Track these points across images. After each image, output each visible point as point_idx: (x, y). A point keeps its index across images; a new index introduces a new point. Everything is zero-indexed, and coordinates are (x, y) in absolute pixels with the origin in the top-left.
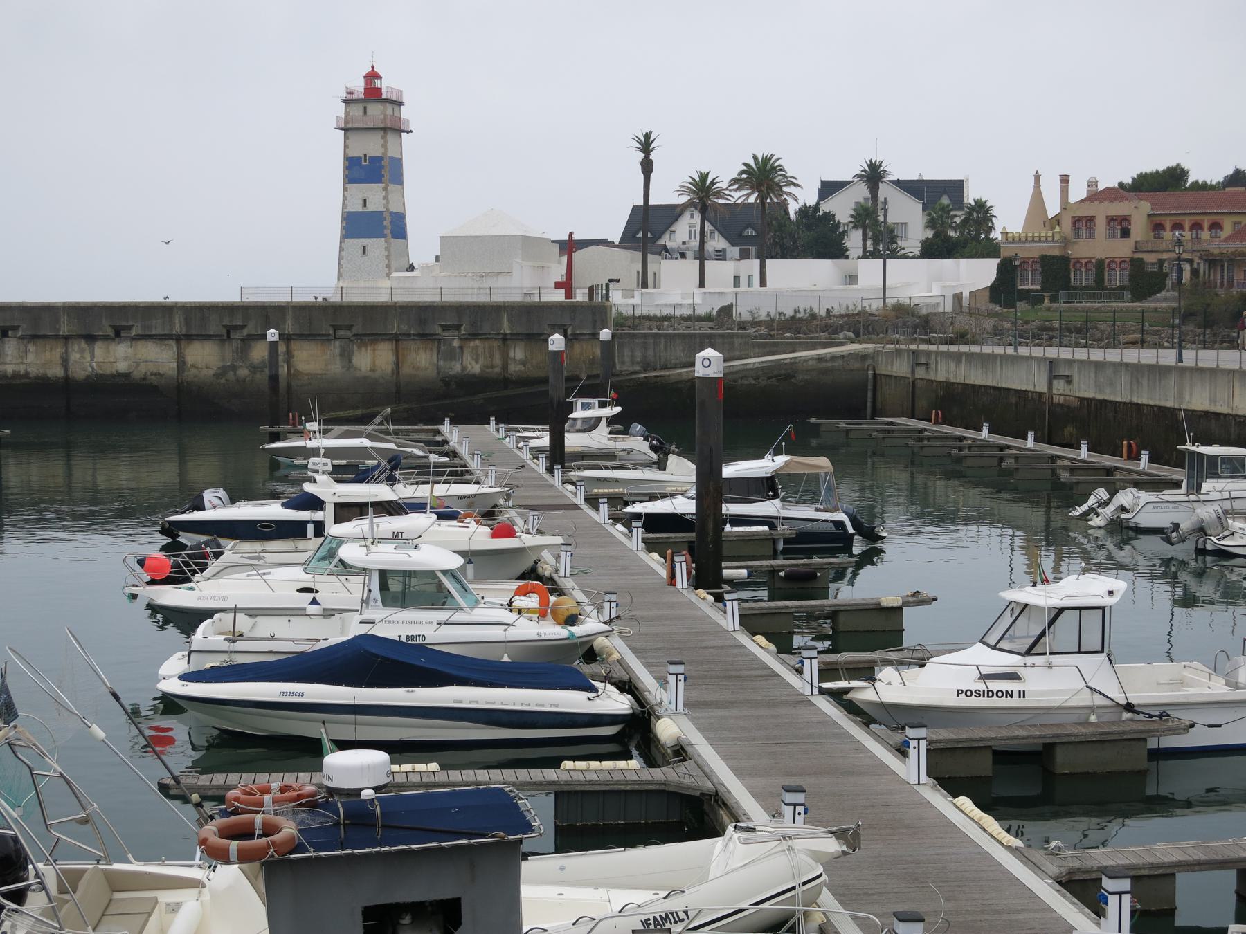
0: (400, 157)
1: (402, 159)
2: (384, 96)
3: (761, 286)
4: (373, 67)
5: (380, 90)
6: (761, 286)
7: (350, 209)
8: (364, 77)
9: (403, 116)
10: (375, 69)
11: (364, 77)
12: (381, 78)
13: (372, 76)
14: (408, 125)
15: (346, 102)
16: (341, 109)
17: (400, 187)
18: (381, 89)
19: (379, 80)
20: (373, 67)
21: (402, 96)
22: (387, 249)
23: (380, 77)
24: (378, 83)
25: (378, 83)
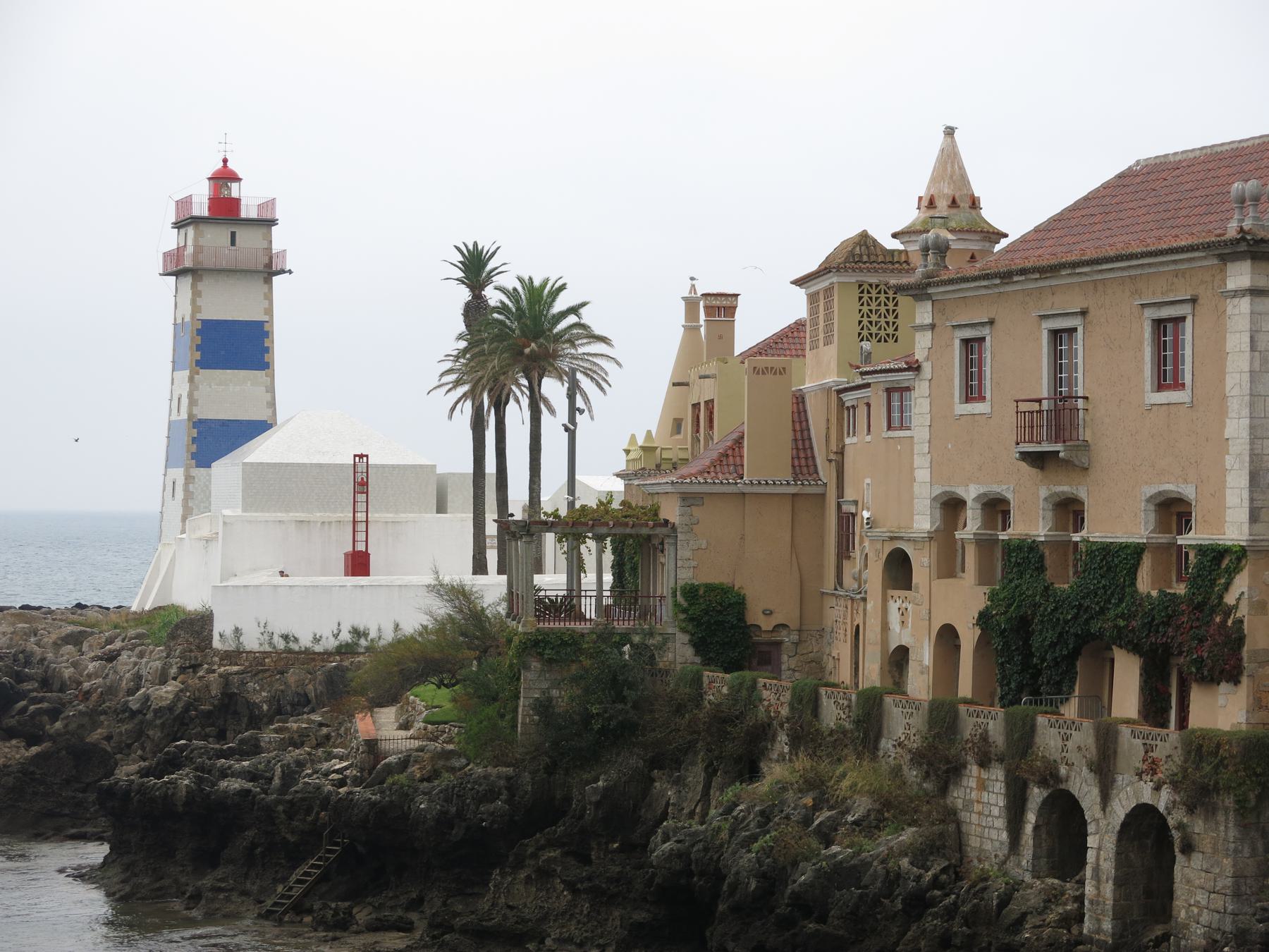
0: (266, 318)
1: (271, 322)
2: (243, 215)
3: (475, 573)
4: (225, 161)
5: (236, 203)
6: (475, 573)
7: (174, 417)
9: (276, 247)
10: (229, 164)
11: (210, 179)
13: (224, 177)
15: (179, 225)
16: (171, 240)
17: (259, 374)
20: (225, 161)
21: (273, 209)
22: (186, 490)
23: (236, 178)
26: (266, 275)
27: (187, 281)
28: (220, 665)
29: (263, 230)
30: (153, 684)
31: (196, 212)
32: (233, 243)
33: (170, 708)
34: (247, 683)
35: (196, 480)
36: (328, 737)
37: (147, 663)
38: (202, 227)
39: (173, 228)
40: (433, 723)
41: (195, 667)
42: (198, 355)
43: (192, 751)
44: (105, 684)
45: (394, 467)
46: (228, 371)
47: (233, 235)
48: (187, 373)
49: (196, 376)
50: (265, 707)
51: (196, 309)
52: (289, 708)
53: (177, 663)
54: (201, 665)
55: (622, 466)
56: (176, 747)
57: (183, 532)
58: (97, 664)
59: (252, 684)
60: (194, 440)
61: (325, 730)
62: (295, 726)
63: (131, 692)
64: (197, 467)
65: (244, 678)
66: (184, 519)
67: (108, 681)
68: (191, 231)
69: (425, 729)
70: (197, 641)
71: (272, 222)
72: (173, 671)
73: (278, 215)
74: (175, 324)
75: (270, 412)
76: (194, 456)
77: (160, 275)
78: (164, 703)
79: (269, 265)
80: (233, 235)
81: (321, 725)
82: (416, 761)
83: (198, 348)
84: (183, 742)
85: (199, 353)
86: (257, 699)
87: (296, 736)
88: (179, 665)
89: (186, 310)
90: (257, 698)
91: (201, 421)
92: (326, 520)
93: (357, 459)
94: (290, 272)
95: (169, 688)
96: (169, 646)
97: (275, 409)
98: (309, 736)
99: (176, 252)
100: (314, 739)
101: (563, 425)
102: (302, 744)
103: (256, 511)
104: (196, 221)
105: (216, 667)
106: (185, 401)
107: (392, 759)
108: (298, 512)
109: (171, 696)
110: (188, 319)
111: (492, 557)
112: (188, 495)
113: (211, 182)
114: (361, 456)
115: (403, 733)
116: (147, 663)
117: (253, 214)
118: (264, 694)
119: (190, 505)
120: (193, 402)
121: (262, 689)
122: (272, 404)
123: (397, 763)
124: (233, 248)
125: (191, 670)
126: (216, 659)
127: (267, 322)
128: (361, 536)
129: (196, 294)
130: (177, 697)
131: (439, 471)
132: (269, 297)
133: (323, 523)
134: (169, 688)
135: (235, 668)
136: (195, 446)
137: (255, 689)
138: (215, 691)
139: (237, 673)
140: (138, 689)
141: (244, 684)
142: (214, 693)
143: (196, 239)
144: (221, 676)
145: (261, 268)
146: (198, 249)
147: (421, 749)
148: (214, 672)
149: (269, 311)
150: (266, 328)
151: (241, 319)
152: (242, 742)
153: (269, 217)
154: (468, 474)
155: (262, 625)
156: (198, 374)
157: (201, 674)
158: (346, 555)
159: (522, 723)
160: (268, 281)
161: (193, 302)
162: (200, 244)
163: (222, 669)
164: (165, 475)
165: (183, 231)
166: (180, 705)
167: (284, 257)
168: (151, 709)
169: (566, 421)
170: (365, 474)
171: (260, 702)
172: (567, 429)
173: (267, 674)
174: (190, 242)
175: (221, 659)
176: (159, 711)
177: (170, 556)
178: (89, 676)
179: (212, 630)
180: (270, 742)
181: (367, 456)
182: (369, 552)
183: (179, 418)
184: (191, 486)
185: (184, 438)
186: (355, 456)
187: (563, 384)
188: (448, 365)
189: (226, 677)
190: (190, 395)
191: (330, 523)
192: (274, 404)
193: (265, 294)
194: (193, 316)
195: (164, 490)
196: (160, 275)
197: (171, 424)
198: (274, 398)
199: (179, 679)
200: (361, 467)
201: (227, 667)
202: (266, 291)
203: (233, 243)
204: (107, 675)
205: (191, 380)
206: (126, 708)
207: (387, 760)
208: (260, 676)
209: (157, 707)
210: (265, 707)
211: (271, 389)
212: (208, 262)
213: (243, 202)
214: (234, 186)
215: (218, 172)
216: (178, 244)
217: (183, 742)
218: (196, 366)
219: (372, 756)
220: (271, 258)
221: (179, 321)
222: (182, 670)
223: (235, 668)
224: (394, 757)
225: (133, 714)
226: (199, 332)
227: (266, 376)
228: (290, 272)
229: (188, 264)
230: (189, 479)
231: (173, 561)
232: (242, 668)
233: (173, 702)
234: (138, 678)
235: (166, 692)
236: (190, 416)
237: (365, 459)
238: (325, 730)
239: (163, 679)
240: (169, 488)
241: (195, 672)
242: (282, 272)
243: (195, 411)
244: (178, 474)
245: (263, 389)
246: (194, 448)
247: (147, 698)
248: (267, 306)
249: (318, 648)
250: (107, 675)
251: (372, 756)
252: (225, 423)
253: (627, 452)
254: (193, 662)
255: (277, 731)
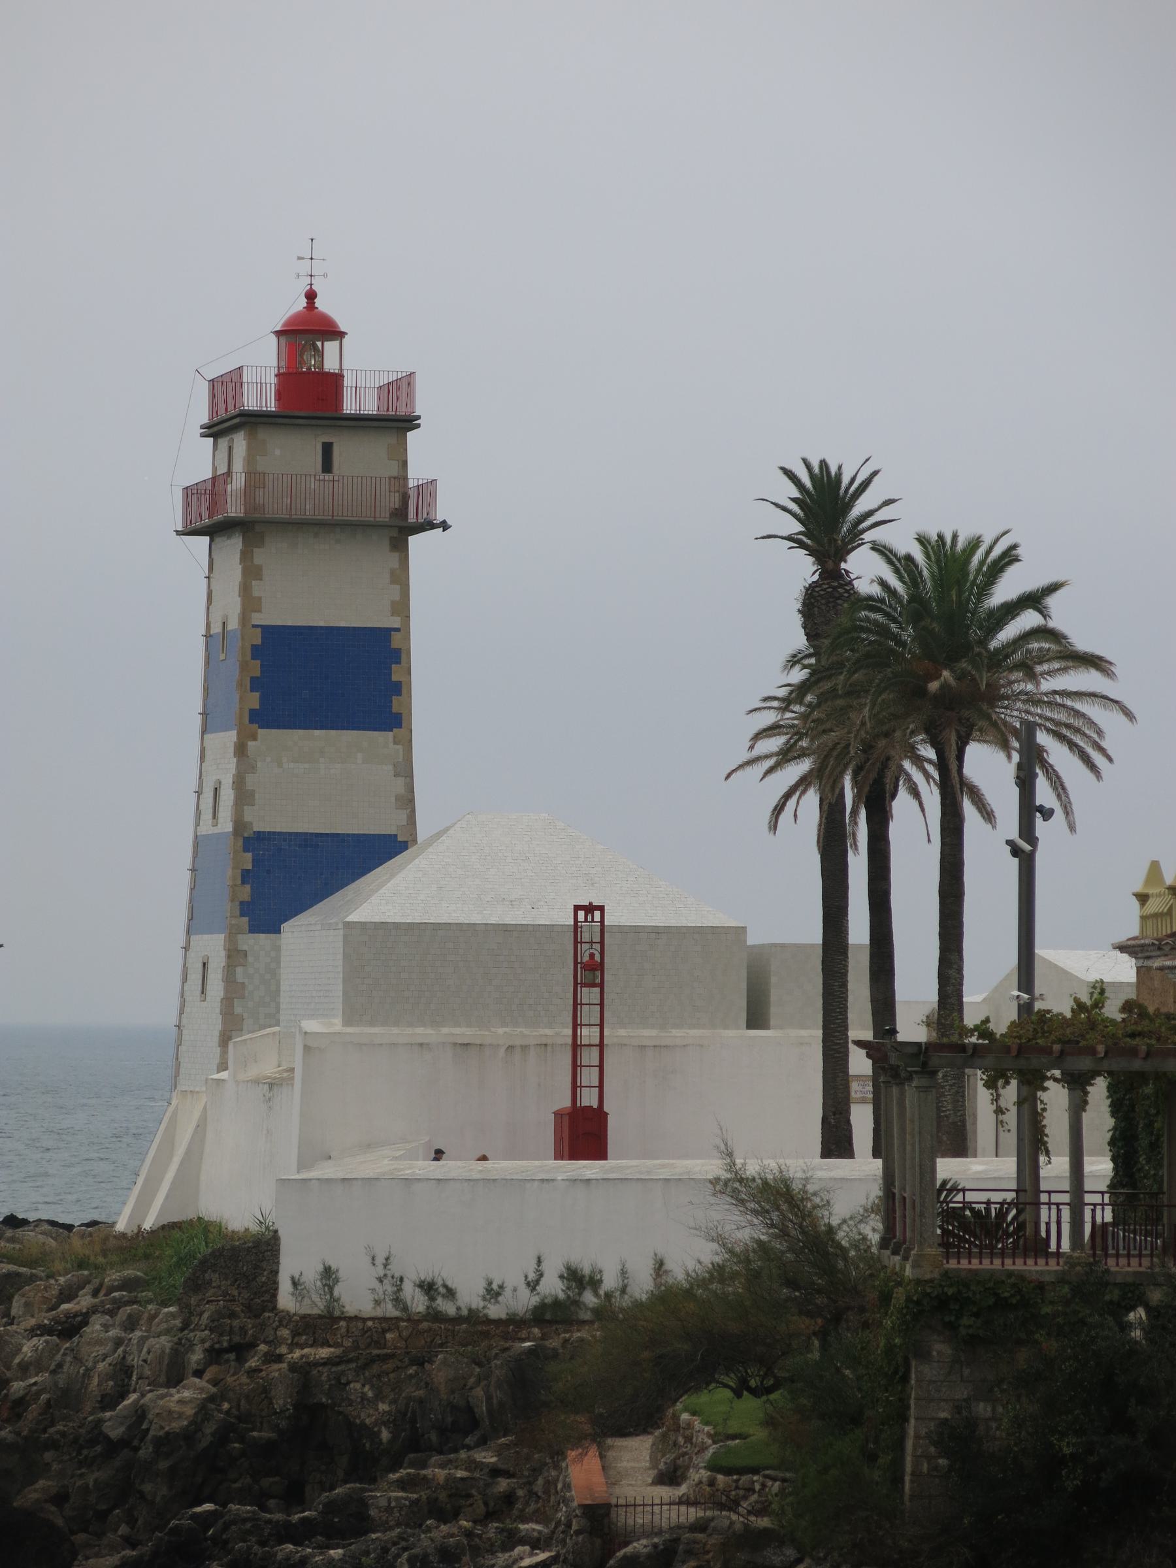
0: (395, 622)
1: (405, 629)
3: (826, 1153)
4: (311, 296)
6: (826, 1153)
7: (206, 828)
8: (279, 334)
9: (416, 474)
10: (318, 303)
11: (279, 334)
12: (338, 335)
14: (432, 504)
15: (216, 430)
18: (336, 380)
19: (336, 344)
20: (311, 296)
21: (410, 395)
23: (333, 332)
24: (331, 356)
25: (331, 356)
26: (395, 533)
27: (233, 545)
28: (293, 1346)
29: (390, 439)
30: (154, 1384)
31: (251, 402)
32: (327, 466)
33: (189, 1436)
34: (348, 1383)
35: (250, 959)
36: (509, 1499)
37: (143, 1340)
38: (263, 434)
39: (203, 435)
40: (728, 1471)
41: (241, 1350)
42: (254, 700)
43: (226, 1527)
44: (56, 1384)
45: (657, 931)
46: (317, 732)
47: (327, 449)
48: (231, 736)
49: (251, 744)
50: (385, 1435)
51: (250, 603)
52: (434, 1437)
53: (203, 1341)
54: (252, 1345)
55: (1130, 928)
56: (194, 1517)
57: (223, 1067)
58: (39, 1342)
59: (358, 1386)
60: (246, 876)
61: (503, 1484)
62: (441, 1474)
63: (109, 1401)
64: (251, 931)
65: (343, 1372)
66: (225, 1040)
67: (62, 1380)
68: (240, 442)
69: (712, 1482)
70: (245, 1294)
71: (409, 423)
72: (196, 1357)
73: (420, 408)
74: (208, 636)
75: (403, 816)
76: (246, 909)
77: (178, 533)
78: (176, 1425)
79: (401, 512)
80: (327, 449)
81: (495, 1472)
82: (690, 1553)
83: (255, 684)
84: (208, 1507)
85: (257, 694)
86: (368, 1417)
87: (443, 1496)
88: (207, 1345)
89: (231, 605)
90: (369, 1416)
91: (261, 837)
92: (518, 1042)
93: (581, 914)
94: (445, 526)
95: (187, 1394)
96: (188, 1306)
97: (413, 811)
98: (469, 1496)
99: (209, 487)
100: (480, 1503)
101: (1009, 842)
102: (456, 1515)
103: (372, 1024)
104: (251, 421)
105: (283, 1350)
106: (228, 796)
107: (640, 1546)
108: (459, 1026)
109: (190, 1411)
110: (233, 624)
111: (862, 1120)
112: (233, 990)
113: (283, 340)
114: (589, 909)
115: (665, 1492)
116: (143, 1340)
117: (370, 406)
118: (383, 1407)
119: (238, 1010)
120: (243, 796)
121: (379, 1396)
122: (407, 801)
123: (649, 1556)
124: (327, 477)
125: (232, 1356)
126: (285, 1333)
127: (398, 630)
128: (589, 1076)
129: (251, 573)
130: (204, 1410)
131: (752, 940)
132: (401, 577)
133: (511, 1048)
134: (187, 1394)
135: (324, 1352)
136: (248, 888)
137: (363, 1397)
138: (281, 1400)
139: (327, 1362)
140: (123, 1396)
141: (340, 1384)
142: (278, 1404)
143: (250, 460)
144: (293, 1367)
145: (384, 516)
146: (255, 480)
147: (700, 1526)
148: (279, 1358)
149: (402, 607)
150: (396, 641)
151: (343, 624)
152: (331, 1507)
153: (402, 411)
154: (812, 946)
155: (380, 1260)
156: (255, 738)
157: (253, 1363)
158: (558, 1115)
159: (913, 1474)
160: (400, 546)
161: (245, 589)
162: (260, 468)
163: (297, 1354)
164: (186, 948)
165: (223, 443)
166: (209, 1429)
167: (433, 495)
168: (149, 1437)
169: (1014, 834)
170: (598, 947)
171: (376, 1423)
172: (1016, 851)
173: (389, 1366)
174: (238, 466)
175: (295, 1334)
176: (165, 1443)
177: (196, 1115)
178: (25, 1369)
179: (277, 1272)
180: (389, 1509)
181: (601, 909)
182: (606, 1109)
183: (216, 830)
184: (239, 970)
185: (224, 873)
186: (577, 908)
187: (1009, 757)
188: (769, 718)
189: (303, 1370)
190: (239, 783)
191: (525, 1048)
192: (412, 801)
193: (393, 573)
194: (244, 618)
195: (185, 980)
196: (178, 533)
197: (198, 843)
198: (411, 789)
199: (208, 1375)
200: (590, 932)
201: (306, 1351)
202: (396, 565)
203: (327, 466)
204: (60, 1365)
205: (241, 750)
206: (97, 1435)
207: (628, 1550)
208: (375, 1369)
209: (161, 1433)
210: (385, 1435)
211: (405, 770)
212: (276, 508)
213: (348, 382)
214: (330, 347)
215: (295, 319)
216: (215, 469)
217: (208, 1507)
218: (251, 721)
219: (598, 1541)
220: (405, 498)
221: (216, 629)
222: (214, 1355)
223: (324, 1352)
224: (644, 1542)
225: (113, 1447)
226: (256, 652)
227: (395, 743)
228: (445, 526)
229: (234, 509)
230: (235, 956)
231: (201, 1128)
232: (336, 1351)
233: (191, 1423)
234: (123, 1371)
235: (181, 1402)
236: (239, 824)
237: (597, 914)
238: (503, 1484)
239: (174, 1375)
240: (195, 977)
241: (241, 1360)
242: (429, 525)
243: (249, 815)
244: (213, 945)
245: (389, 769)
246: (246, 892)
247: (140, 1413)
248: (397, 598)
249: (495, 1311)
250: (60, 1365)
251: (598, 1541)
252: (309, 841)
253: (1143, 898)
254: (237, 1339)
255: (403, 1485)
